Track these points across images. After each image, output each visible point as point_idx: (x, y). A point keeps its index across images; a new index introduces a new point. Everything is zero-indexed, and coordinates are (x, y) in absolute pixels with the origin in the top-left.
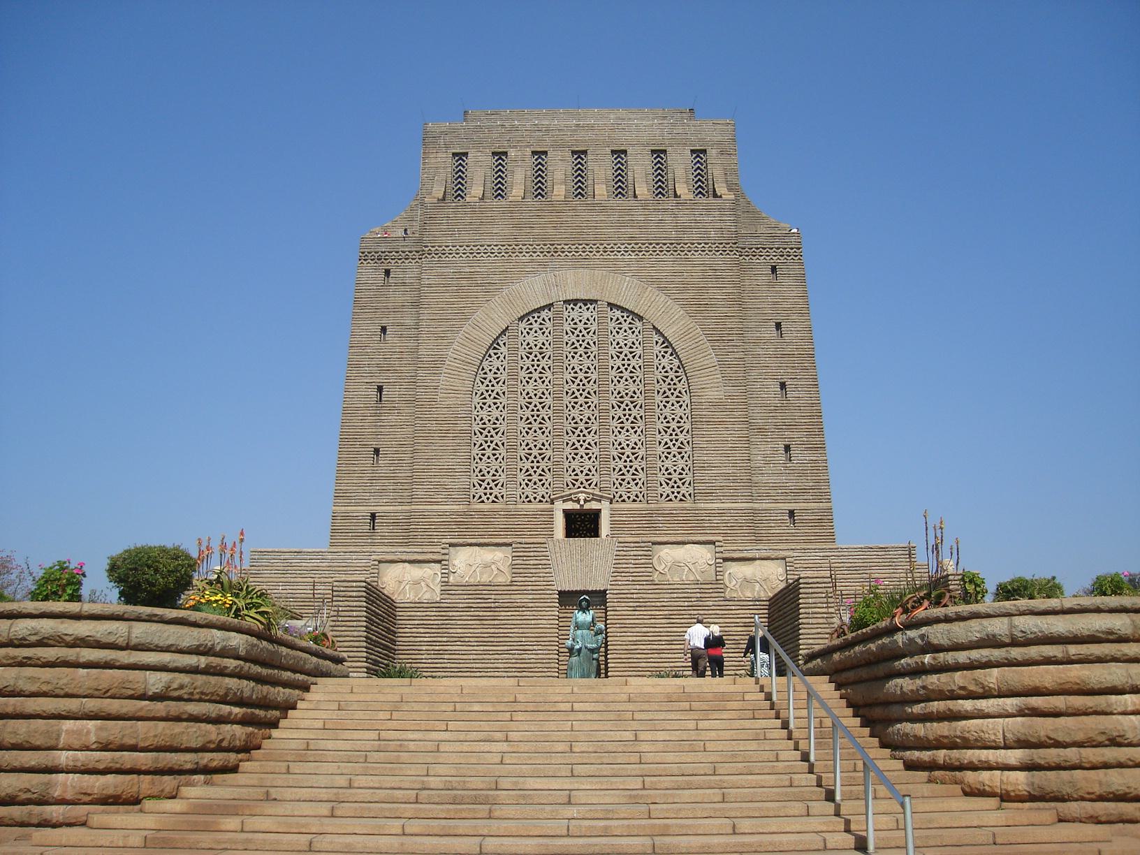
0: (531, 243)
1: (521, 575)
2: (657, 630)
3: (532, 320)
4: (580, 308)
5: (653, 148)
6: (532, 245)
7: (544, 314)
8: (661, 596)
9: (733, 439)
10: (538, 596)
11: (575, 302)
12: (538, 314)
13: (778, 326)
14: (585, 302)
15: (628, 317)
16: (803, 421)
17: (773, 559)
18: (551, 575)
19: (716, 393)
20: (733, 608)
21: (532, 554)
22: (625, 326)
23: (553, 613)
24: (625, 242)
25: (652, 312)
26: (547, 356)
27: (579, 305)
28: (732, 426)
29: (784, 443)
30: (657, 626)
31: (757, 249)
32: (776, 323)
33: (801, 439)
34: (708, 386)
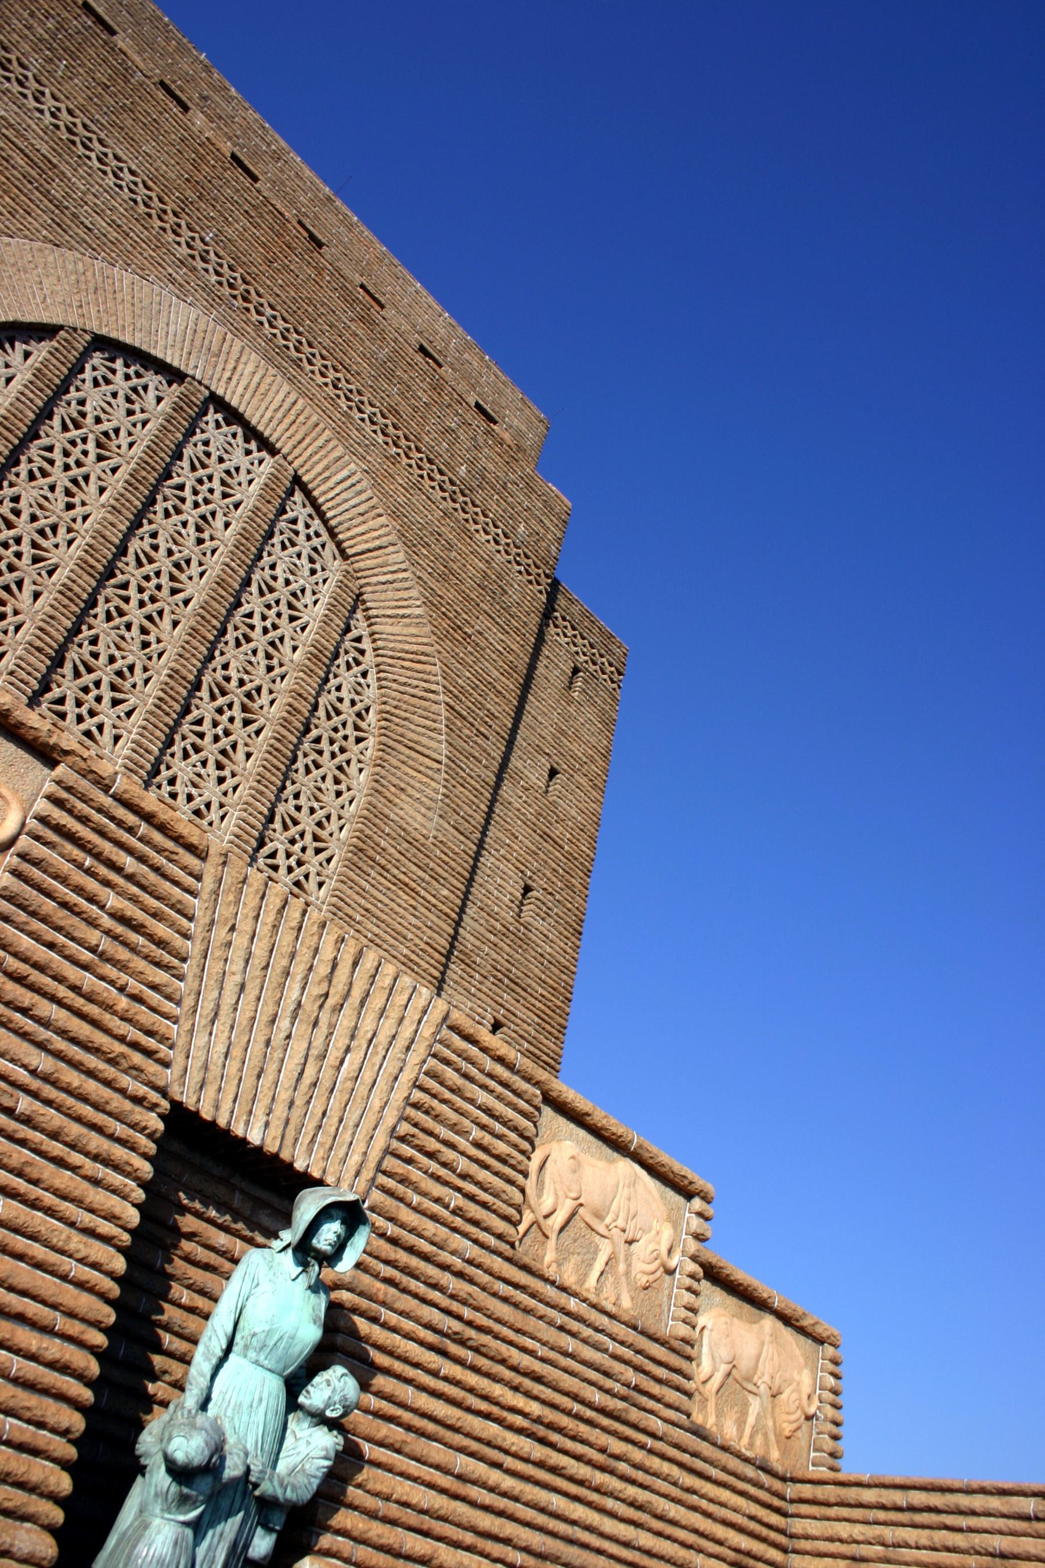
0: (207, 239)
1: (37, 925)
2: (508, 1483)
3: (119, 364)
4: (234, 436)
5: (425, 345)
6: (206, 244)
7: (152, 379)
8: (531, 1324)
9: (418, 941)
10: (73, 1078)
11: (233, 416)
12: (142, 371)
13: (553, 773)
14: (252, 433)
15: (317, 535)
16: (540, 990)
17: (802, 1331)
18: (168, 1006)
19: (420, 818)
20: (714, 1472)
21: (129, 863)
22: (304, 547)
23: (114, 1203)
24: (378, 404)
25: (369, 563)
26: (112, 463)
27: (234, 428)
28: (423, 910)
29: (495, 1014)
30: (509, 1462)
31: (564, 619)
32: (552, 767)
33: (525, 1026)
34: (410, 791)
